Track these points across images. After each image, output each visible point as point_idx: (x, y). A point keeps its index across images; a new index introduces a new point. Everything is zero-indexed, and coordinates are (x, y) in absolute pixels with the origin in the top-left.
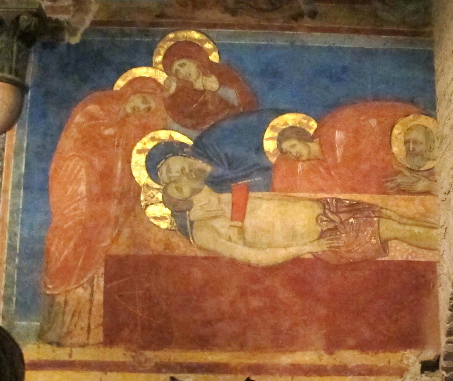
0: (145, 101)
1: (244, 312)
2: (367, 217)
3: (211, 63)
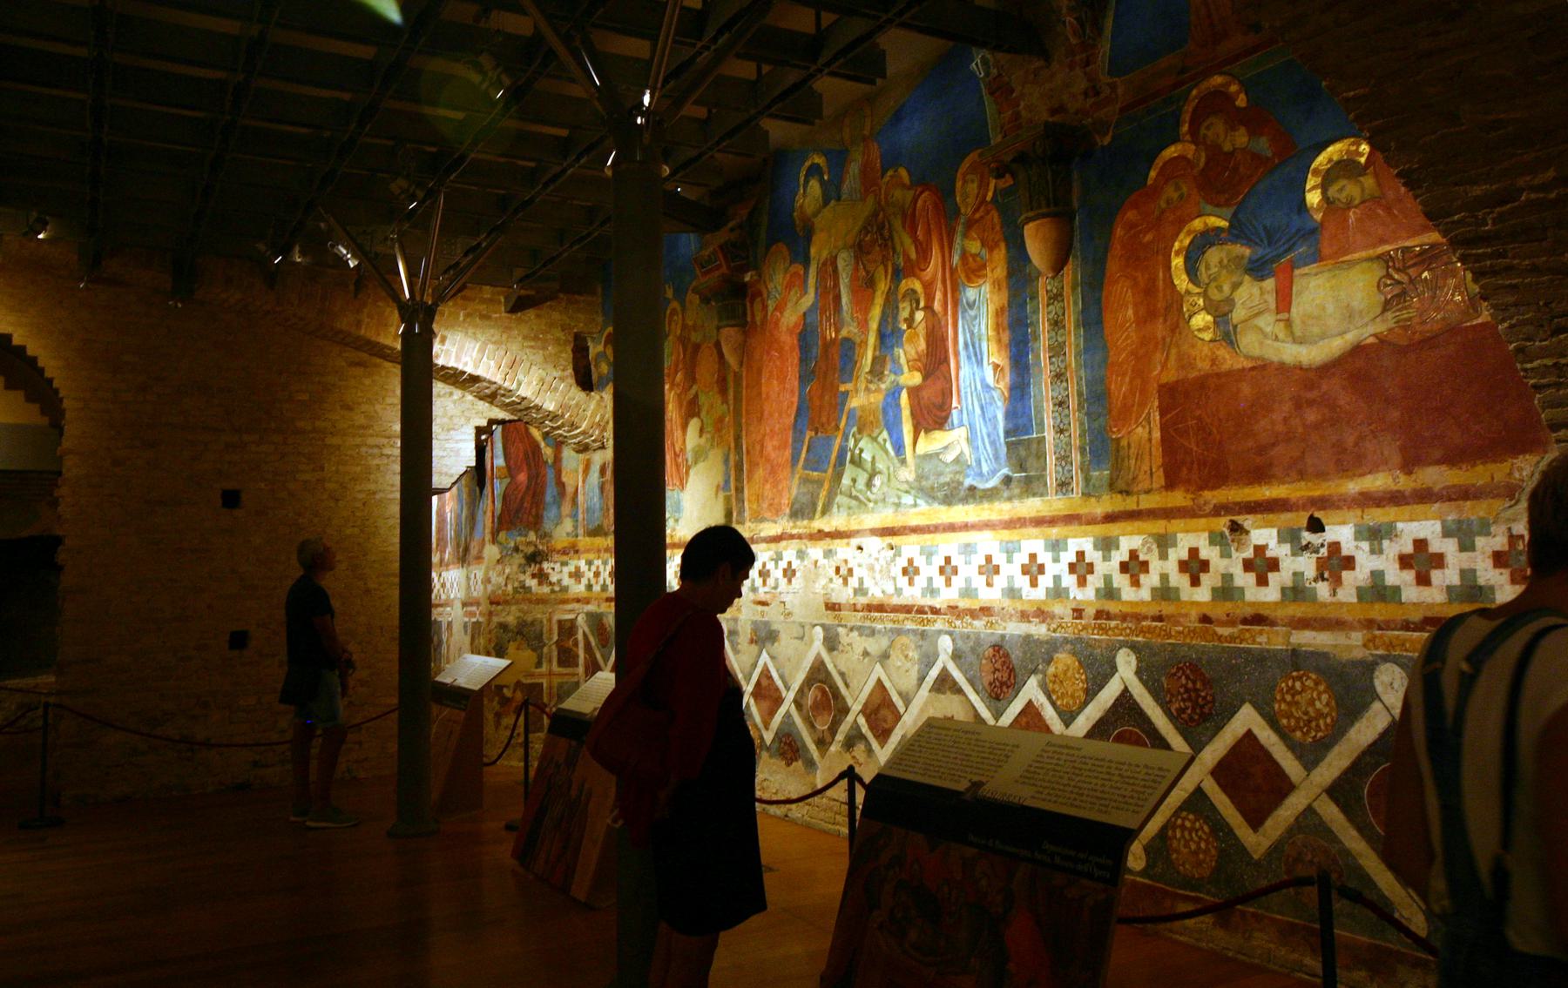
0: (1178, 188)
1: (1300, 430)
2: (1446, 264)
3: (1238, 109)
